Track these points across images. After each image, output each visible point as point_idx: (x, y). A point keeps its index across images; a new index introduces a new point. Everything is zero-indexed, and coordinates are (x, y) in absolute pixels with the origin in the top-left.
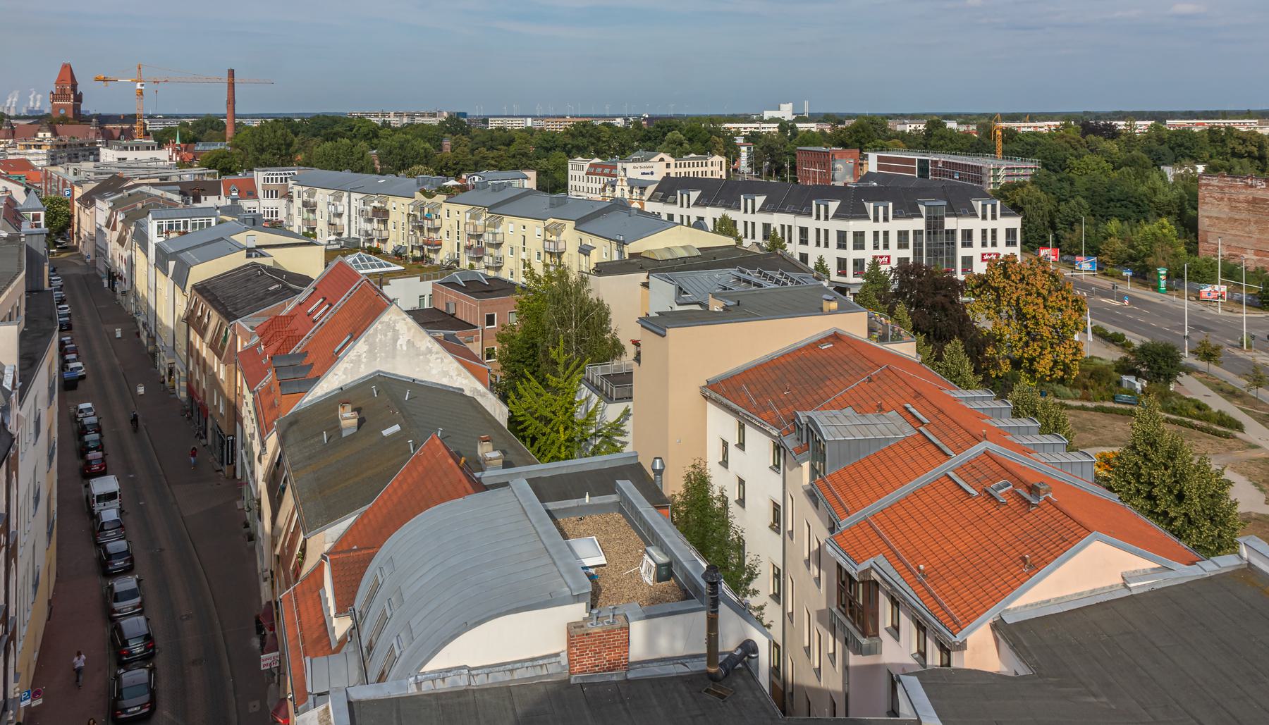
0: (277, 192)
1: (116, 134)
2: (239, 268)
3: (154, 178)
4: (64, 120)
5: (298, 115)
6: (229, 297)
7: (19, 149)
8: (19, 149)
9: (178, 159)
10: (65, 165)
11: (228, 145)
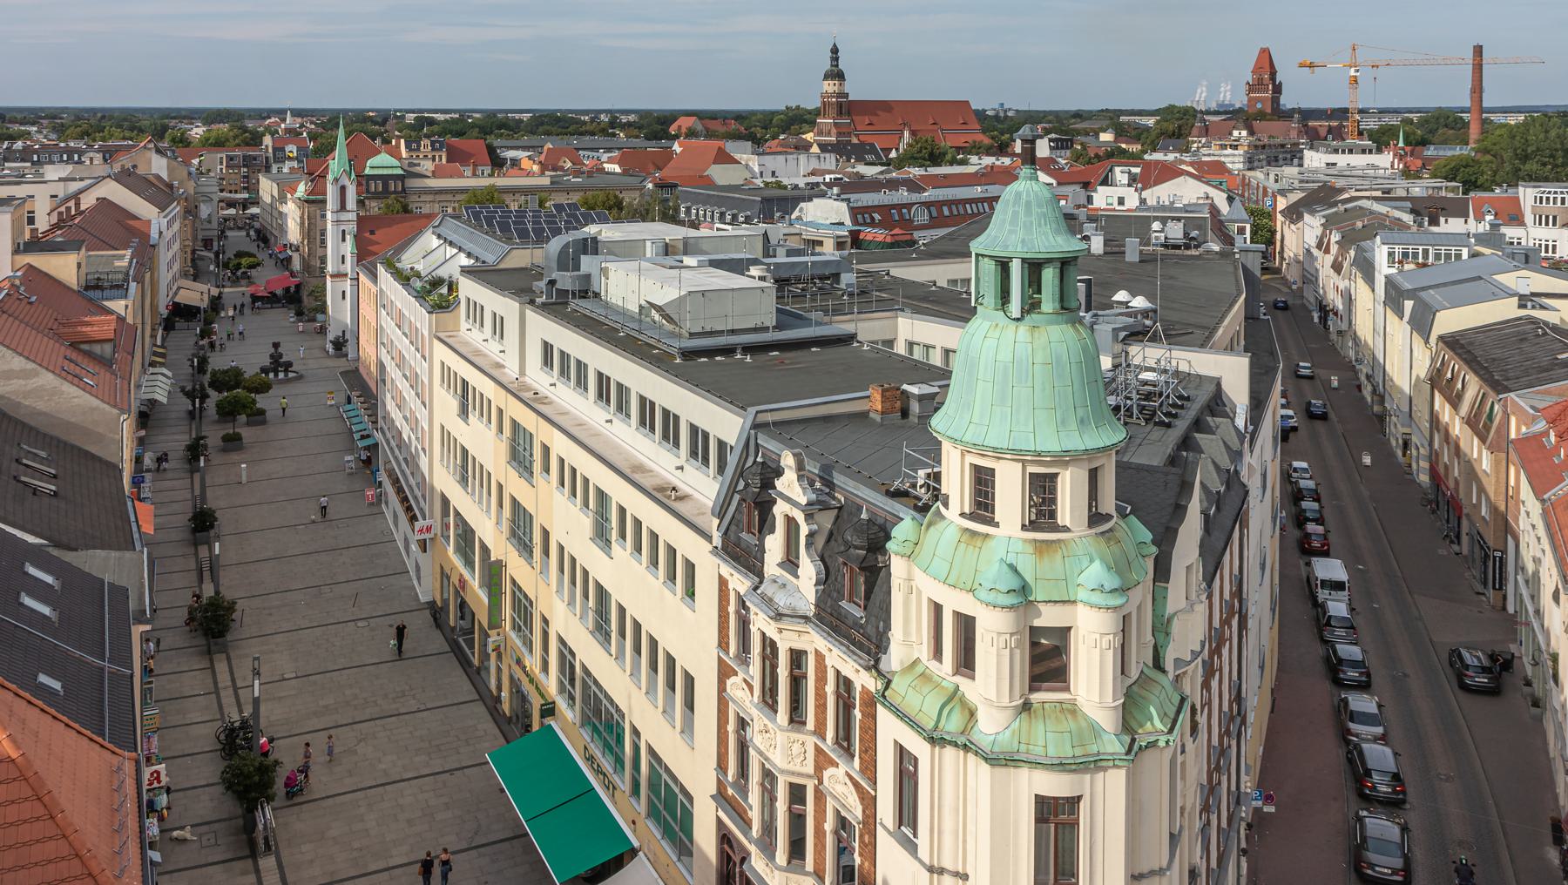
0: (1555, 218)
1: (1323, 132)
4: (1261, 116)
8: (1214, 150)
9: (1401, 166)
10: (1265, 170)
11: (1472, 149)
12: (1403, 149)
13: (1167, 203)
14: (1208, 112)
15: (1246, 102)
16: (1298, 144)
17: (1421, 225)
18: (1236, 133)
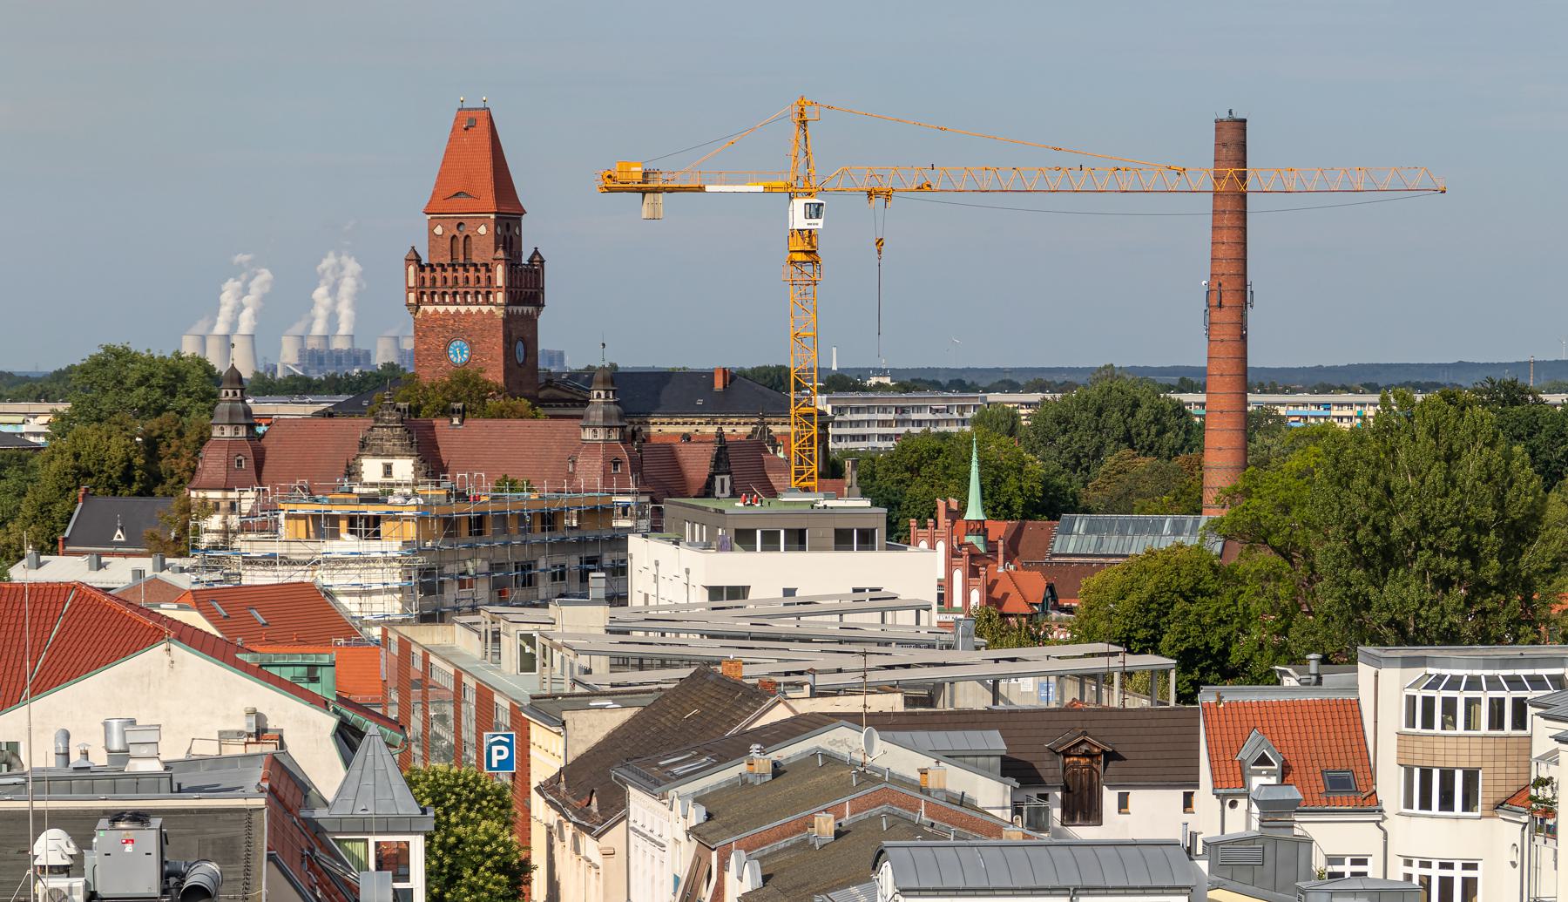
0: (1471, 777)
1: (697, 463)
3: (883, 689)
7: (290, 539)
8: (290, 539)
9: (975, 597)
10: (484, 617)
11: (1214, 526)
12: (980, 529)
13: (99, 759)
14: (267, 386)
15: (408, 344)
16: (608, 512)
17: (1037, 822)
18: (372, 469)
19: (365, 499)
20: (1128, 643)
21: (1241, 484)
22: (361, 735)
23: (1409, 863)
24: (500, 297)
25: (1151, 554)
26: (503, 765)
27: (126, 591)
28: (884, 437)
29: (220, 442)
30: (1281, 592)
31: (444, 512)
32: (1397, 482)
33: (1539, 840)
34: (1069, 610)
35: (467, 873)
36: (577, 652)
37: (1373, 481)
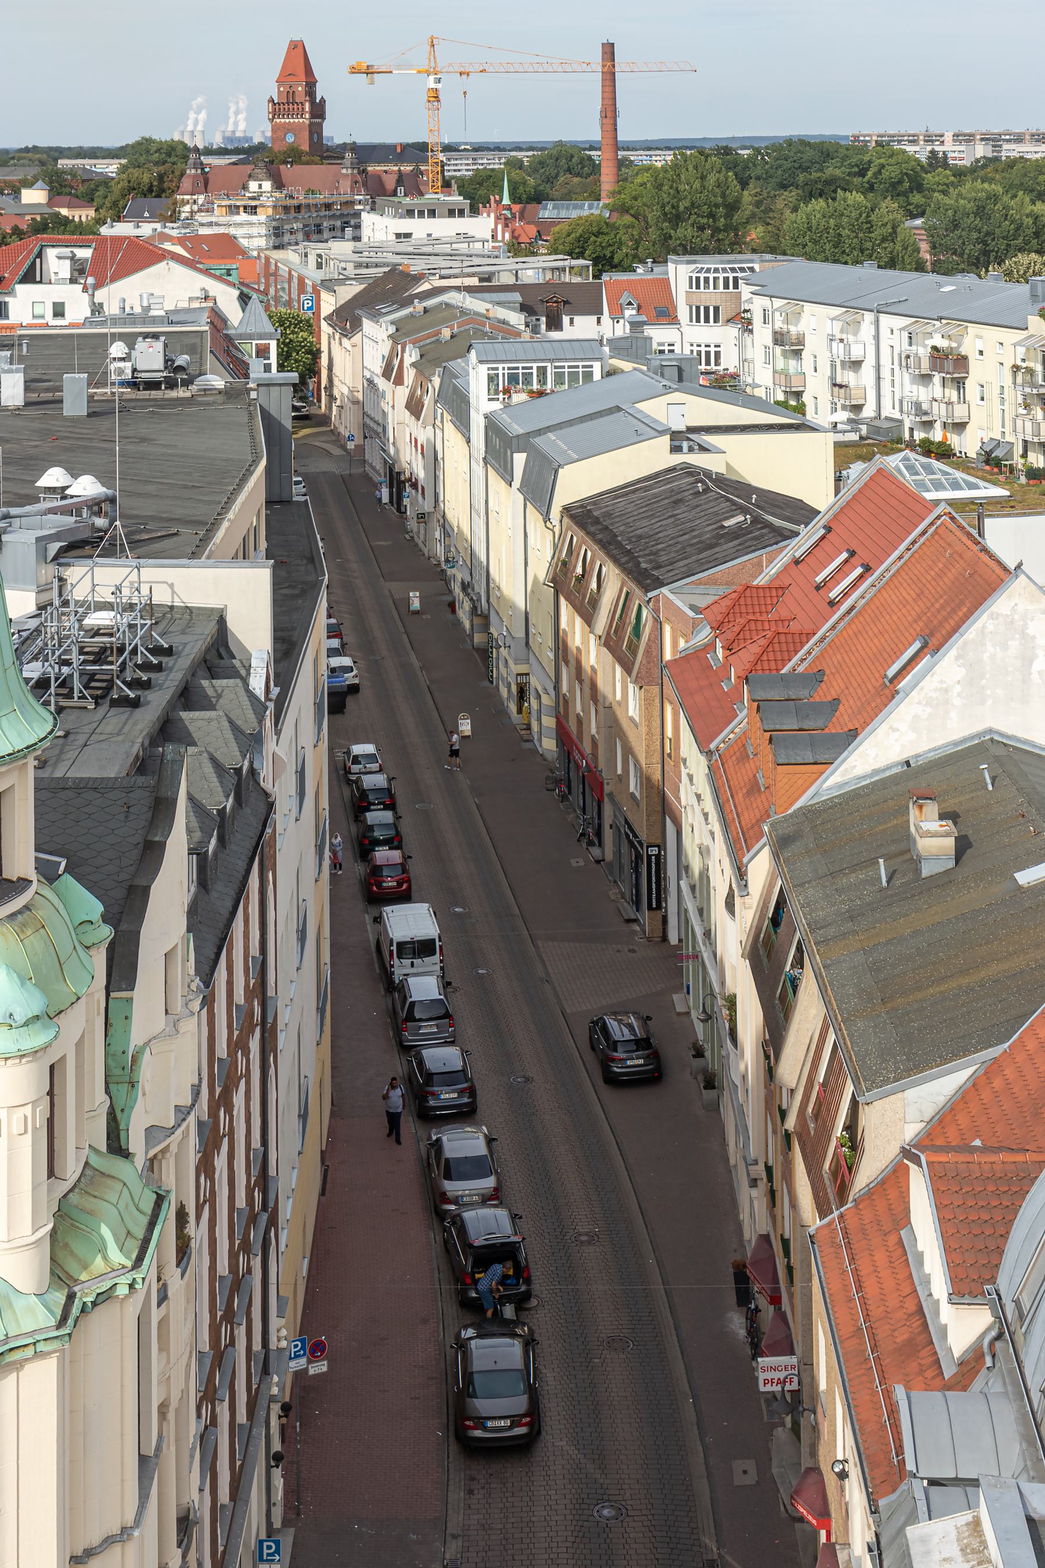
0: (716, 309)
1: (390, 182)
2: (657, 475)
4: (294, 156)
5: (746, 142)
6: (640, 537)
7: (219, 215)
8: (219, 215)
9: (507, 236)
10: (301, 247)
11: (606, 206)
13: (138, 310)
14: (209, 152)
15: (269, 134)
16: (353, 203)
17: (535, 330)
18: (253, 186)
19: (250, 198)
20: (571, 254)
21: (617, 189)
22: (250, 298)
23: (692, 345)
24: (307, 116)
25: (580, 218)
26: (309, 309)
27: (149, 238)
28: (467, 170)
29: (189, 176)
30: (635, 233)
31: (284, 203)
32: (681, 187)
33: (746, 335)
34: (546, 241)
35: (294, 354)
36: (340, 261)
37: (671, 188)
